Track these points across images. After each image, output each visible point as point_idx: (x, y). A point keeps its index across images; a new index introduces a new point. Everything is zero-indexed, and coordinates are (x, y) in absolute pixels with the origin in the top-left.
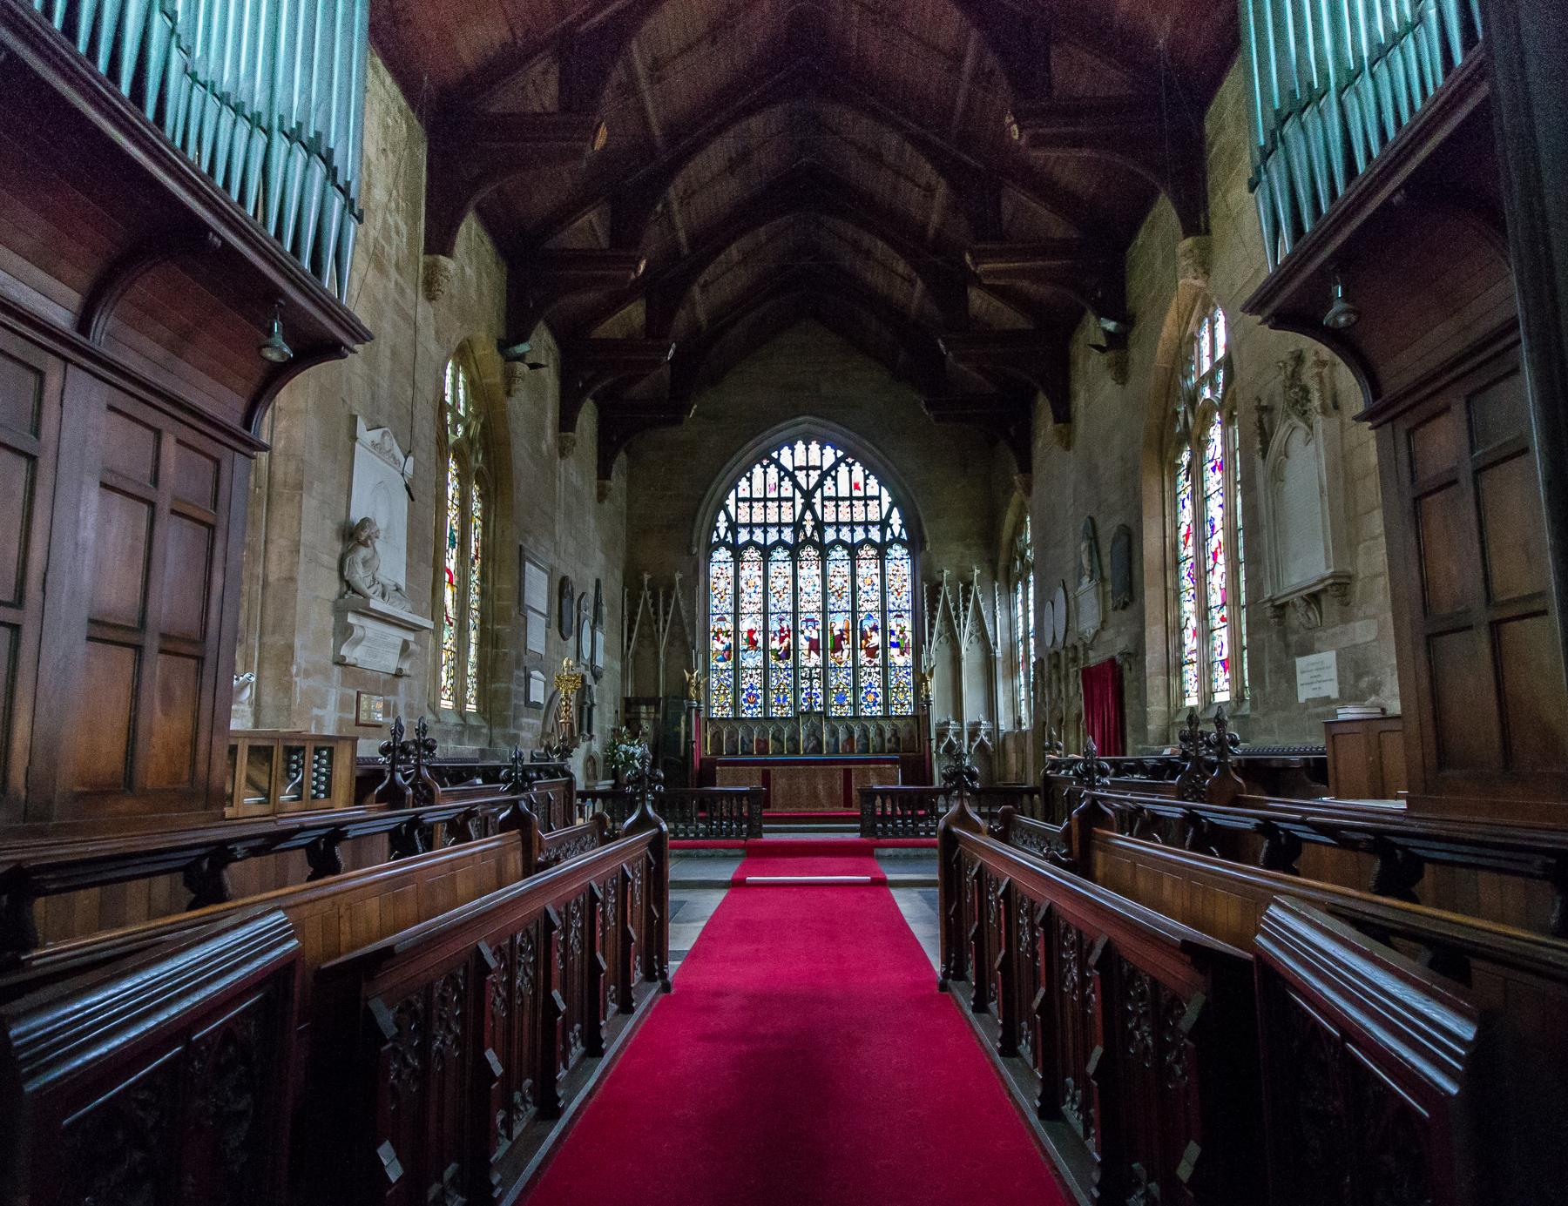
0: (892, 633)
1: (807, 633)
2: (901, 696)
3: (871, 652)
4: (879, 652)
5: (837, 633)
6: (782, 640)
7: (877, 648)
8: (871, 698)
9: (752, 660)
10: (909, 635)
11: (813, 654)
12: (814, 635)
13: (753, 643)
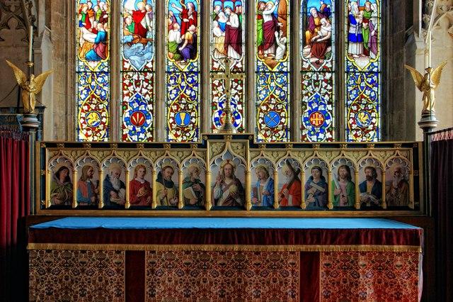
0: (352, 19)
1: (222, 20)
2: (362, 118)
3: (320, 49)
4: (332, 49)
5: (267, 19)
6: (184, 29)
7: (328, 43)
8: (317, 120)
9: (136, 58)
10: (377, 24)
11: (232, 53)
12: (234, 22)
13: (141, 32)
